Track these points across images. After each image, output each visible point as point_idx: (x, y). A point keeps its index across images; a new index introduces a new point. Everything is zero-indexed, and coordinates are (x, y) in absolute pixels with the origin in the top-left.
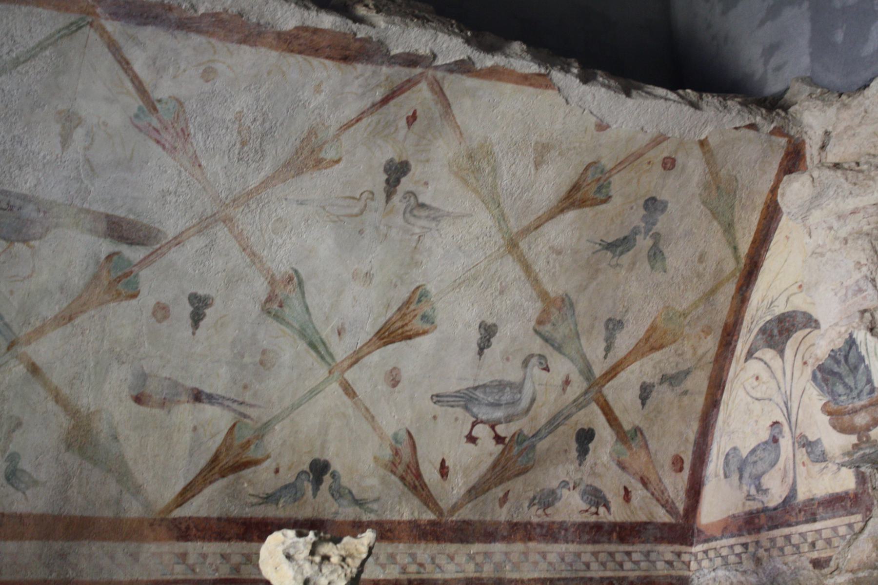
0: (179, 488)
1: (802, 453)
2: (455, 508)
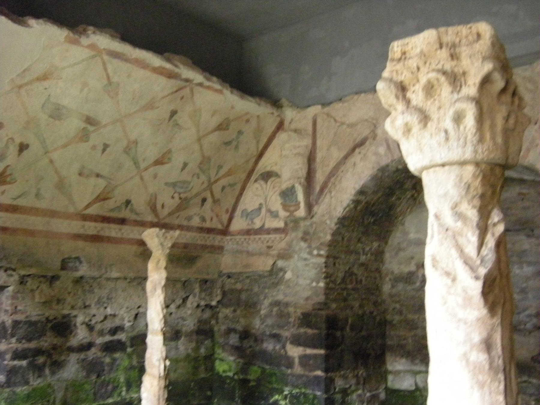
0: (86, 203)
1: (268, 214)
2: (164, 218)
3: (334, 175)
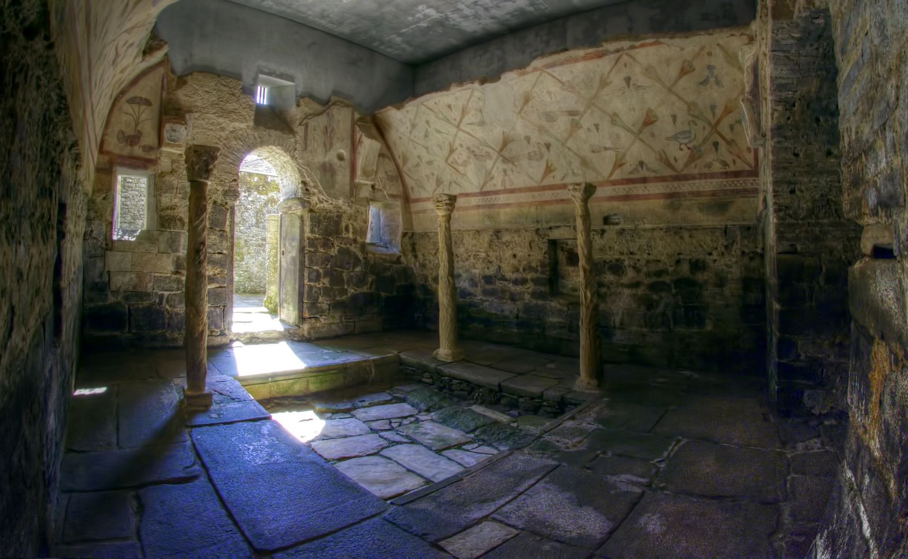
0: (609, 172)
2: (682, 170)
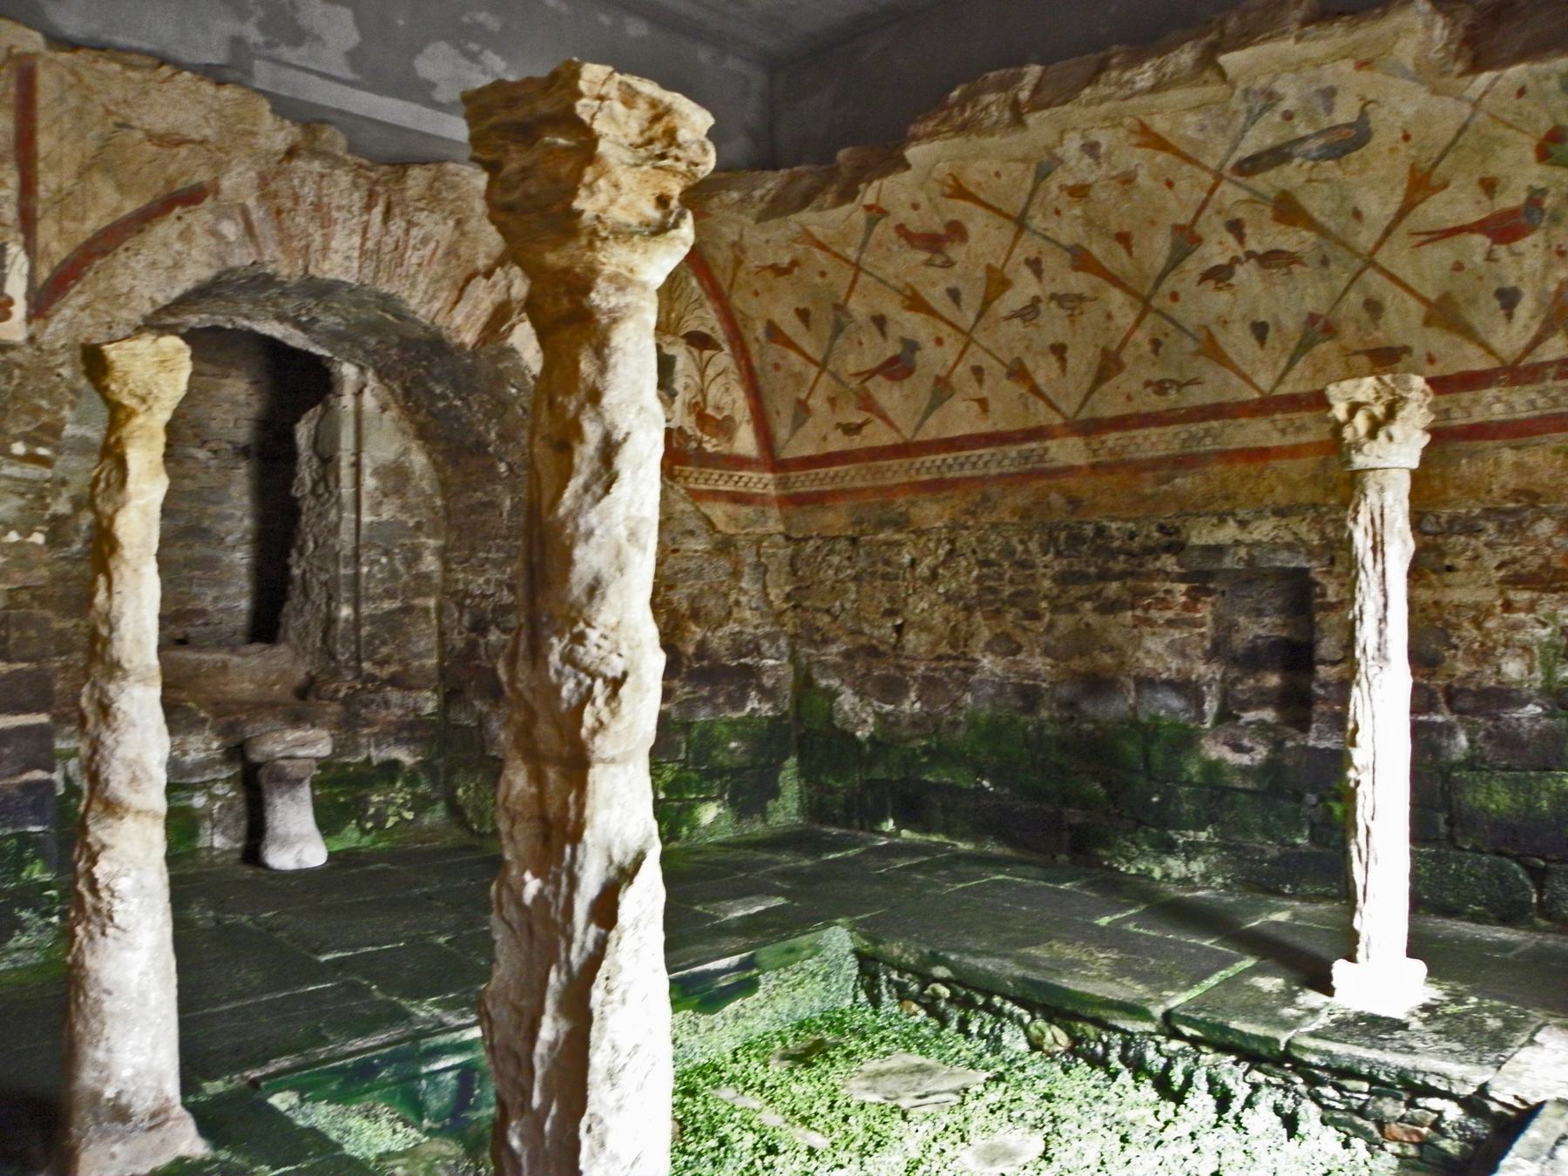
3: (104, 253)
